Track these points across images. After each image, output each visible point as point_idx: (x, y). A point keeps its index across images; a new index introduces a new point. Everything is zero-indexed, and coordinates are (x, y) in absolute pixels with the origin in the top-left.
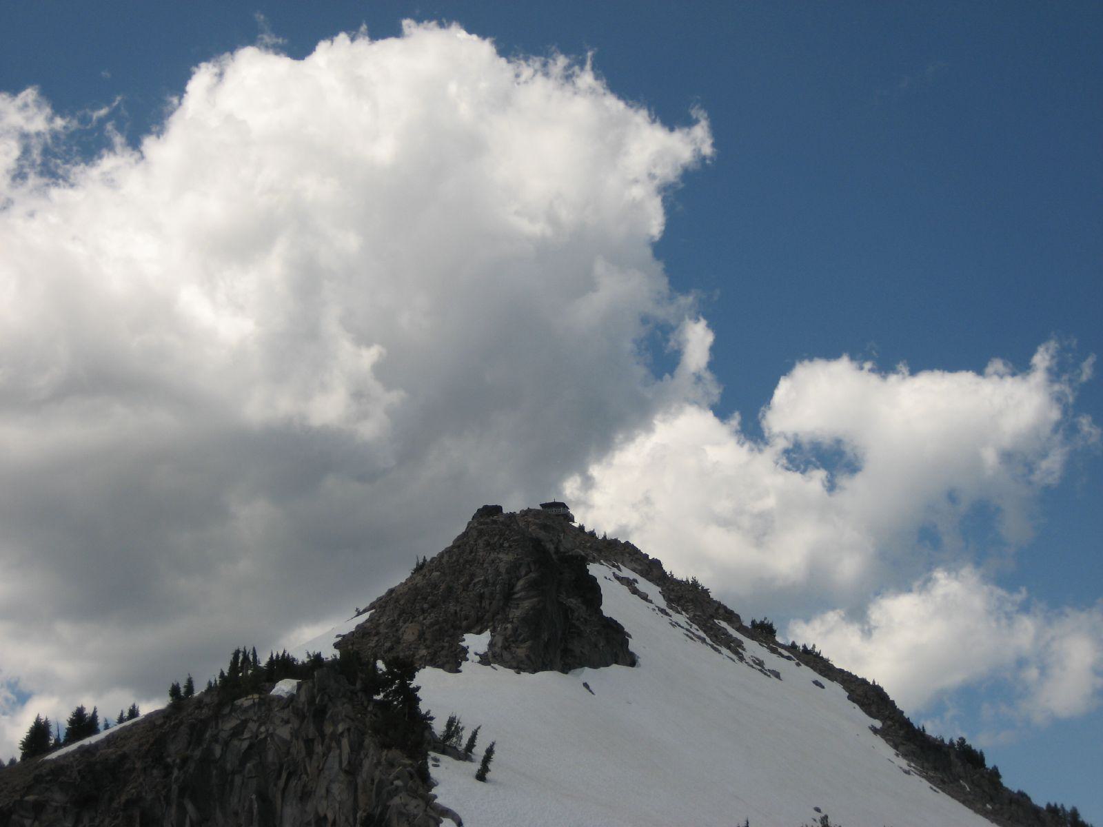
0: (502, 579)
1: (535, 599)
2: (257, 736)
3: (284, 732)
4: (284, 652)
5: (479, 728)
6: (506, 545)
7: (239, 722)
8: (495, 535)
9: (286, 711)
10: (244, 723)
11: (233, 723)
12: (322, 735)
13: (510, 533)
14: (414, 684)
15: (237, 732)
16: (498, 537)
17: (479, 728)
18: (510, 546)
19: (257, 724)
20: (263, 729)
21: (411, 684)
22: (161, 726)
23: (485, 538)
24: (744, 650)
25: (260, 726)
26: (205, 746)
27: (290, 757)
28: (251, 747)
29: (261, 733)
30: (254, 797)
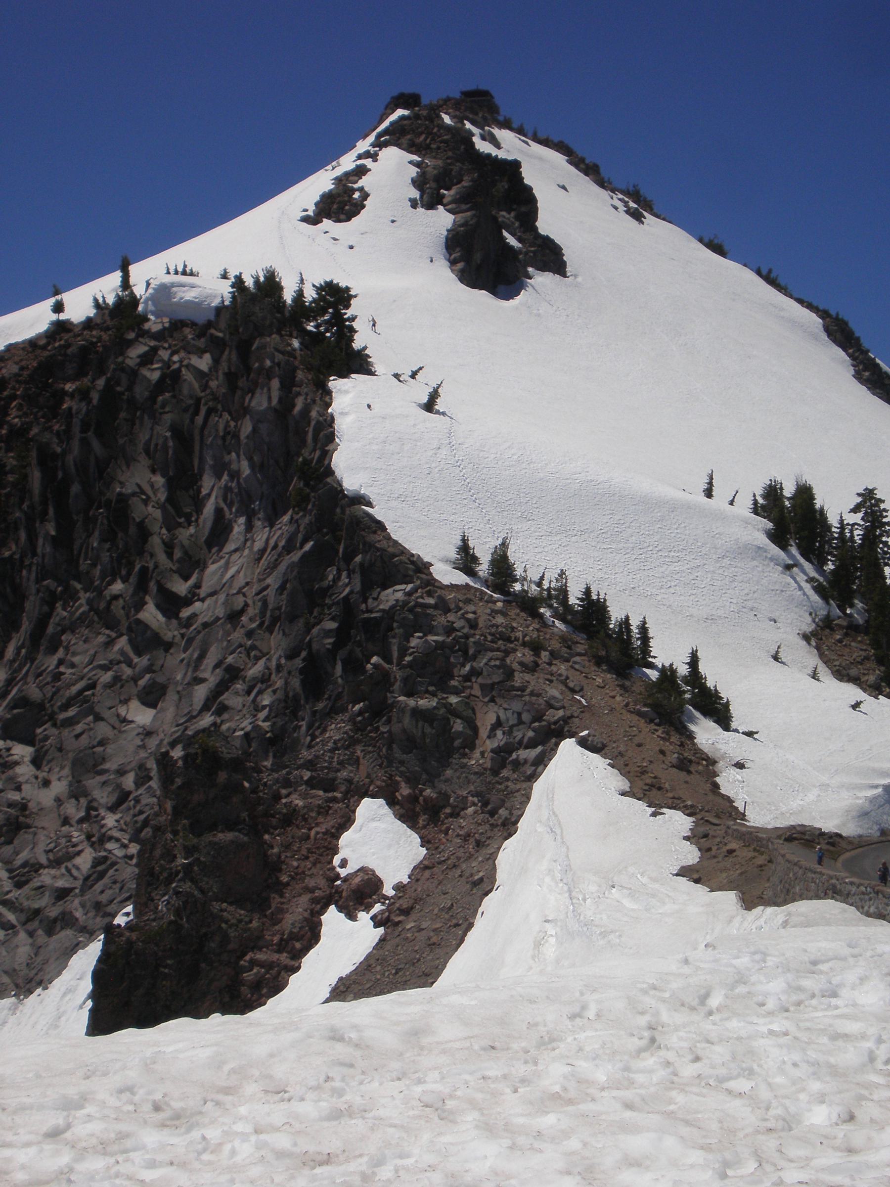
0: (430, 188)
1: (469, 214)
2: (169, 367)
3: (204, 363)
4: (185, 266)
5: (421, 368)
6: (434, 146)
7: (146, 348)
8: (422, 133)
9: (203, 340)
10: (154, 350)
11: (141, 349)
12: (248, 369)
13: (439, 131)
14: (349, 313)
15: (147, 359)
16: (423, 136)
17: (421, 368)
18: (439, 148)
19: (169, 352)
20: (176, 358)
21: (346, 314)
22: (44, 348)
23: (409, 137)
24: (411, 162)
25: (172, 354)
26: (109, 375)
27: (208, 391)
28: (162, 379)
29: (175, 362)
30: (168, 434)
